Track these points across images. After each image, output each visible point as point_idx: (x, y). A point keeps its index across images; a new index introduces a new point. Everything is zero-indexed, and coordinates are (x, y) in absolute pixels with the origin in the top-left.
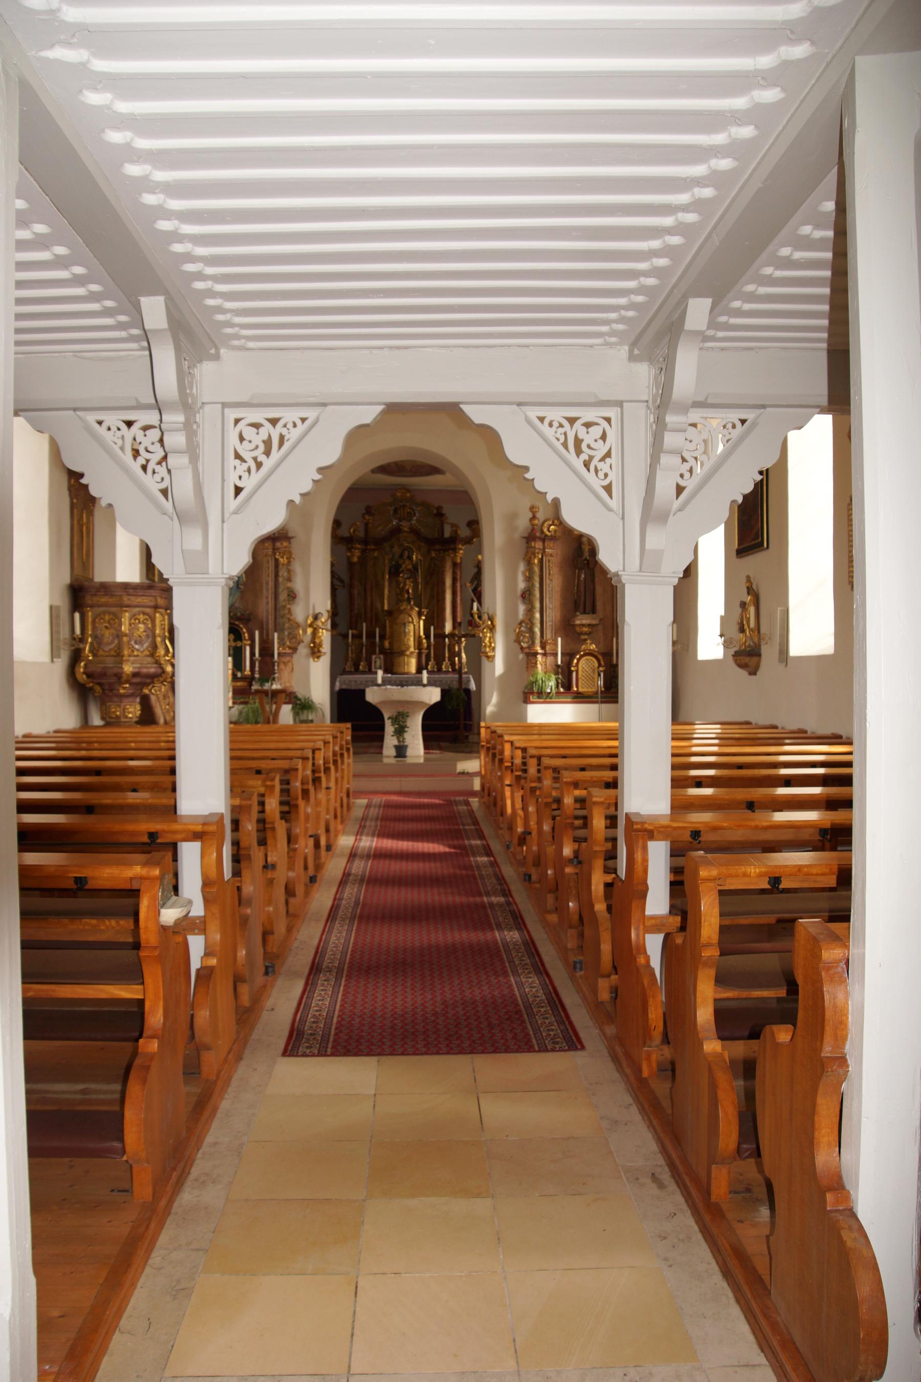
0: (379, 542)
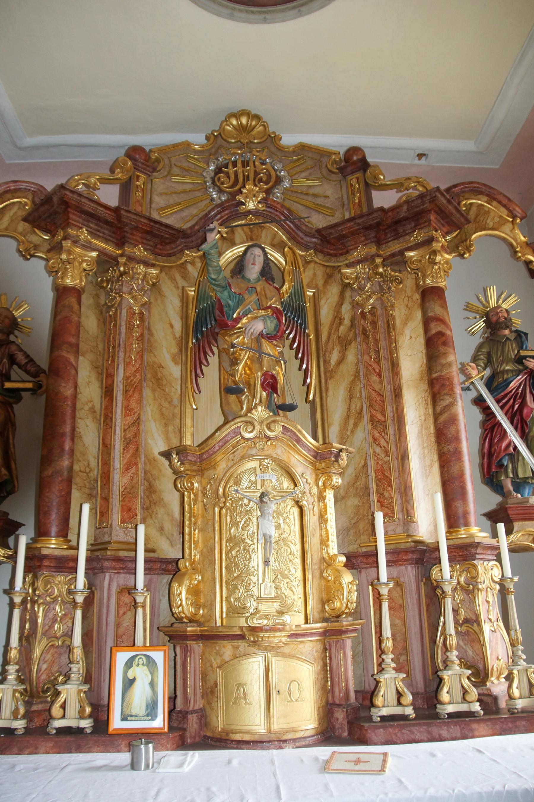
0: (166, 241)
